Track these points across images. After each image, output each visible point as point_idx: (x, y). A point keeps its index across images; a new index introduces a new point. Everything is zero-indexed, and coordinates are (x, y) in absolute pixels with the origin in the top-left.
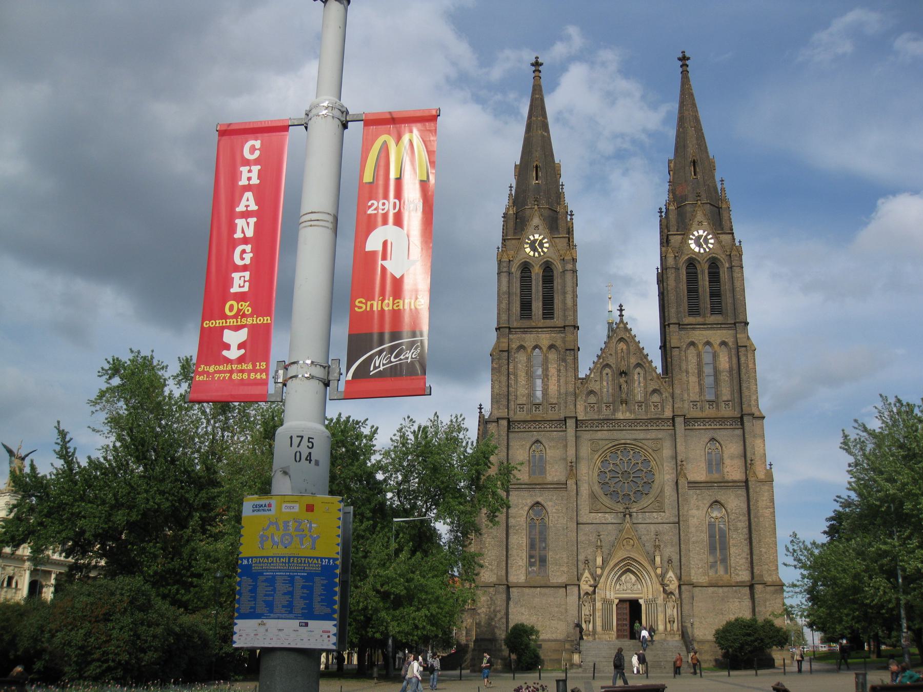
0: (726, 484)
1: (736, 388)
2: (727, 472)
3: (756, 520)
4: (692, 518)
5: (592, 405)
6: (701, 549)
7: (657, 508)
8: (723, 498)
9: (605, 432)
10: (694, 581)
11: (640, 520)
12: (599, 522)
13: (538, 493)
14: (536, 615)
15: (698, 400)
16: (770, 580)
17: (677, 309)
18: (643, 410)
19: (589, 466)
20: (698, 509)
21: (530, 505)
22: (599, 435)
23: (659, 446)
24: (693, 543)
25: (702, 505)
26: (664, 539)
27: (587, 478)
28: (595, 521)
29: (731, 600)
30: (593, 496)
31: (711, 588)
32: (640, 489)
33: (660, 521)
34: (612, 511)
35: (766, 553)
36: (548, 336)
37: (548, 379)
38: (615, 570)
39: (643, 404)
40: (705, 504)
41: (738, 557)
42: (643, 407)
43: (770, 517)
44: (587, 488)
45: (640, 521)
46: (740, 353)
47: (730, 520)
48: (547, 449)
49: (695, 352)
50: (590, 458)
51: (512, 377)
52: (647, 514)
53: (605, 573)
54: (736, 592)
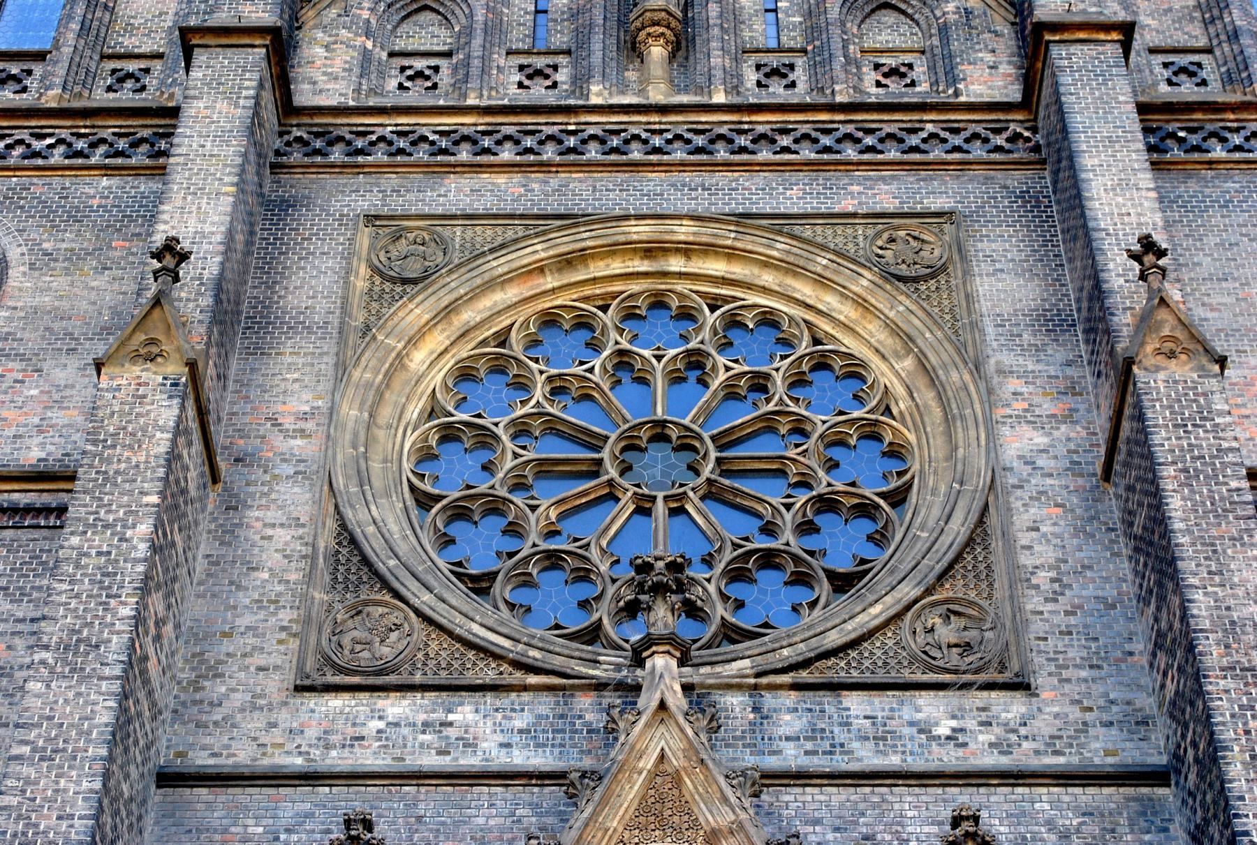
5: (420, 64)
7: (954, 658)
9: (501, 179)
11: (790, 749)
12: (369, 759)
15: (1202, 42)
18: (802, 87)
19: (342, 369)
23: (934, 253)
28: (337, 760)
32: (787, 538)
33: (992, 760)
34: (518, 677)
39: (800, 62)
44: (304, 512)
45: (791, 757)
50: (359, 318)
52: (855, 703)
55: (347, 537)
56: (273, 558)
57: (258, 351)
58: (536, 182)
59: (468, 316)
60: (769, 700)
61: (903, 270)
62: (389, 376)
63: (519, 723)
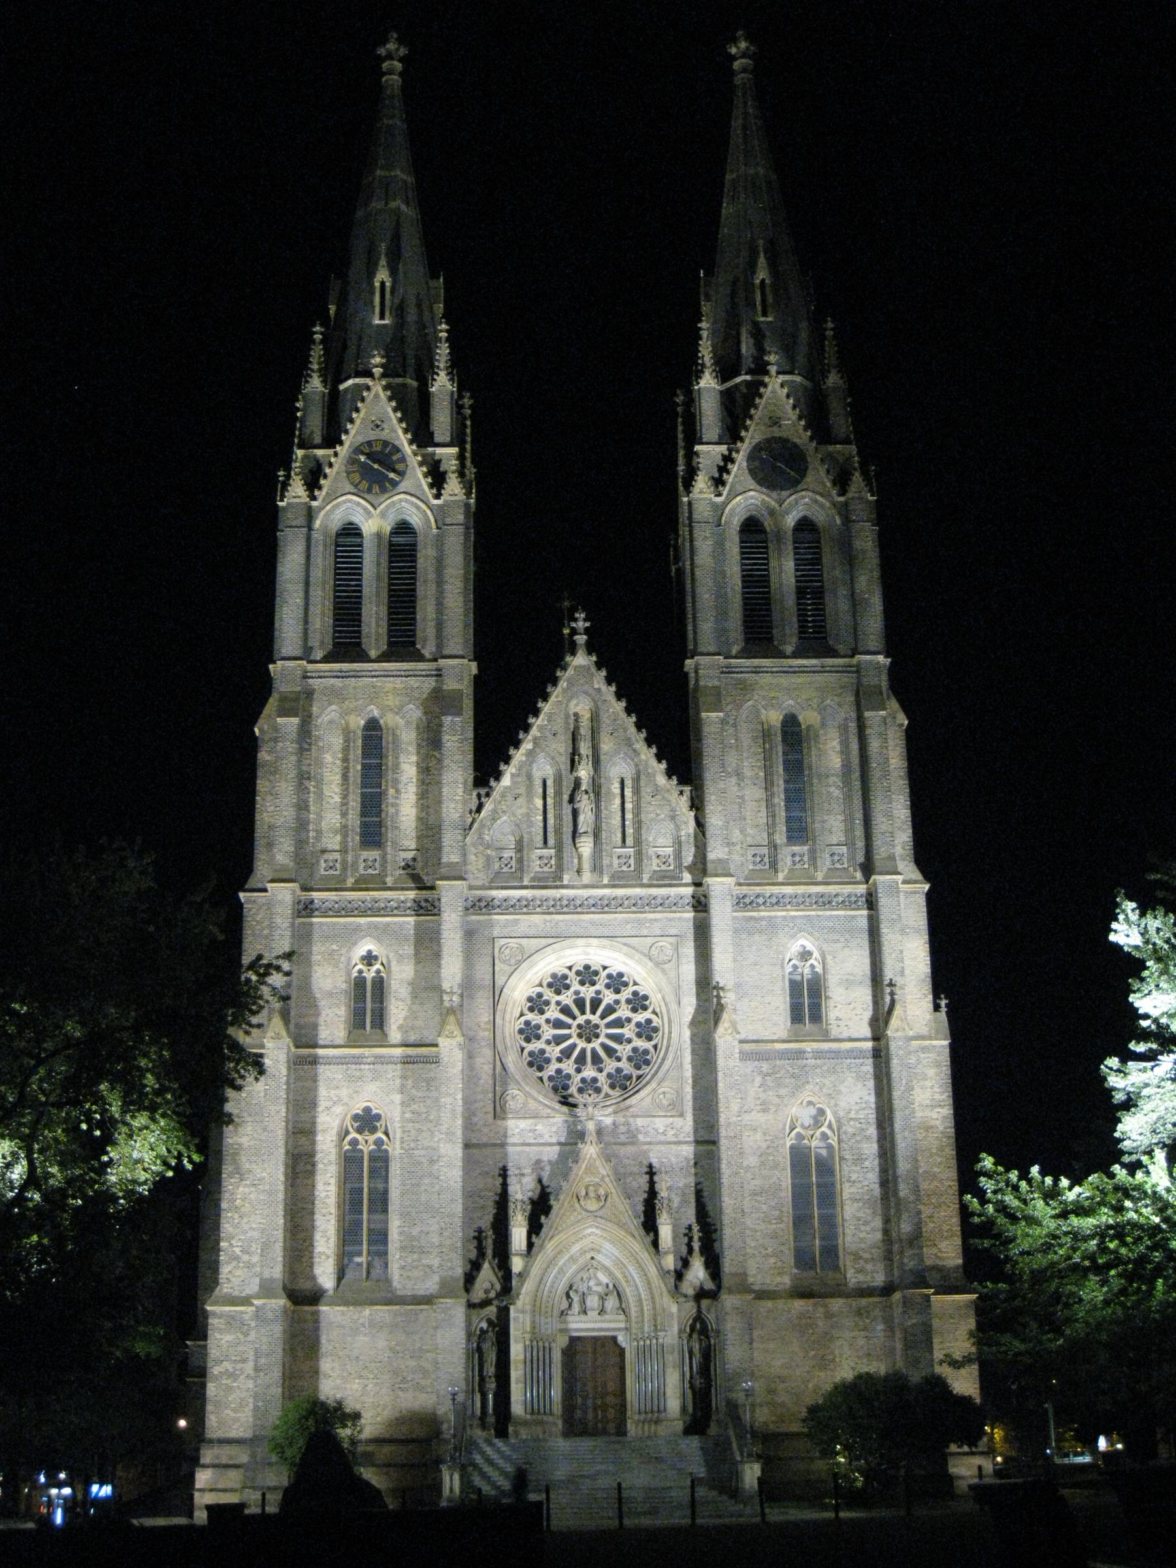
1: (859, 815)
2: (838, 1019)
4: (751, 1133)
14: (360, 1377)
17: (717, 621)
20: (764, 1111)
24: (754, 1194)
25: (776, 1100)
27: (487, 1034)
35: (931, 1217)
36: (398, 683)
37: (398, 791)
41: (863, 1228)
42: (632, 861)
46: (868, 731)
47: (844, 1137)
48: (394, 963)
53: (535, 1271)
56: (484, 1076)
57: (471, 997)
63: (554, 1129)
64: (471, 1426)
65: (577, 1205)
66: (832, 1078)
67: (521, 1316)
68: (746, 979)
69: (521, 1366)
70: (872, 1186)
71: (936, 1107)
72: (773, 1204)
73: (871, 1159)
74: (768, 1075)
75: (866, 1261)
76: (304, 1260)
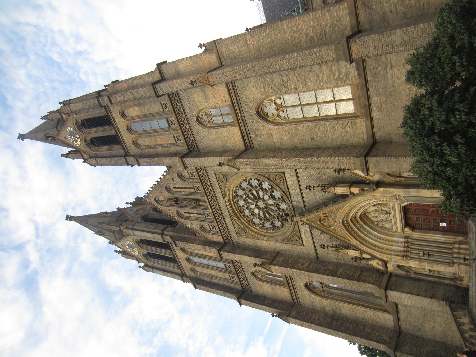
0: (236, 103)
2: (222, 102)
3: (256, 68)
6: (319, 130)
8: (251, 106)
9: (227, 222)
10: (365, 137)
12: (311, 239)
13: (296, 284)
16: (348, 19)
20: (272, 135)
21: (308, 292)
22: (230, 226)
25: (266, 130)
26: (316, 175)
28: (311, 242)
29: (390, 82)
30: (287, 240)
31: (374, 114)
33: (295, 177)
38: (363, 235)
40: (264, 127)
41: (321, 78)
43: (257, 37)
45: (300, 198)
49: (140, 139)
51: (213, 280)
52: (291, 191)
54: (375, 75)
55: (283, 240)
58: (226, 218)
59: (247, 224)
60: (293, 200)
61: (225, 179)
62: (259, 234)
64: (460, 284)
65: (332, 228)
66: (249, 102)
67: (393, 259)
68: (220, 144)
69: (423, 264)
70: (296, 75)
71: (247, 43)
72: (316, 129)
73: (282, 77)
74: (255, 134)
75: (340, 74)
76: (377, 321)
